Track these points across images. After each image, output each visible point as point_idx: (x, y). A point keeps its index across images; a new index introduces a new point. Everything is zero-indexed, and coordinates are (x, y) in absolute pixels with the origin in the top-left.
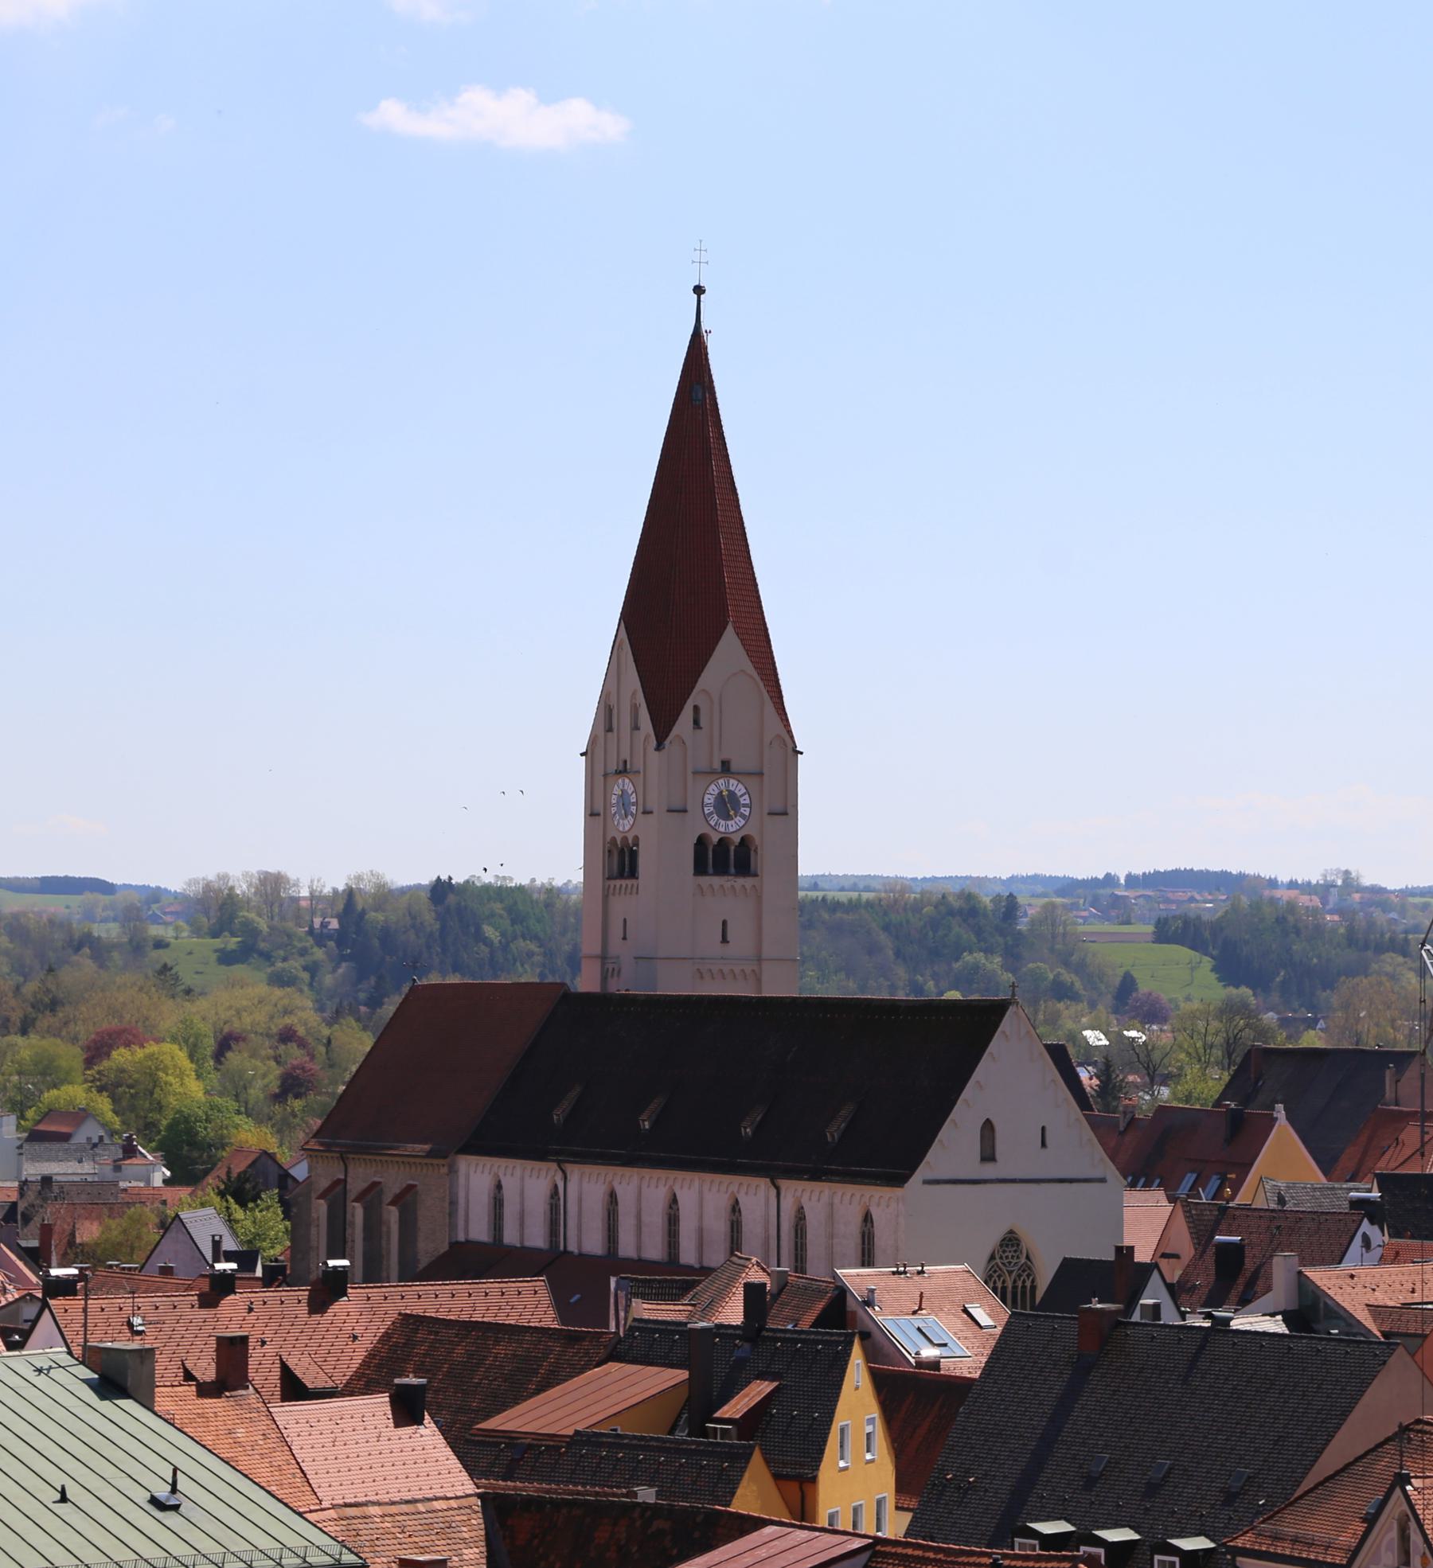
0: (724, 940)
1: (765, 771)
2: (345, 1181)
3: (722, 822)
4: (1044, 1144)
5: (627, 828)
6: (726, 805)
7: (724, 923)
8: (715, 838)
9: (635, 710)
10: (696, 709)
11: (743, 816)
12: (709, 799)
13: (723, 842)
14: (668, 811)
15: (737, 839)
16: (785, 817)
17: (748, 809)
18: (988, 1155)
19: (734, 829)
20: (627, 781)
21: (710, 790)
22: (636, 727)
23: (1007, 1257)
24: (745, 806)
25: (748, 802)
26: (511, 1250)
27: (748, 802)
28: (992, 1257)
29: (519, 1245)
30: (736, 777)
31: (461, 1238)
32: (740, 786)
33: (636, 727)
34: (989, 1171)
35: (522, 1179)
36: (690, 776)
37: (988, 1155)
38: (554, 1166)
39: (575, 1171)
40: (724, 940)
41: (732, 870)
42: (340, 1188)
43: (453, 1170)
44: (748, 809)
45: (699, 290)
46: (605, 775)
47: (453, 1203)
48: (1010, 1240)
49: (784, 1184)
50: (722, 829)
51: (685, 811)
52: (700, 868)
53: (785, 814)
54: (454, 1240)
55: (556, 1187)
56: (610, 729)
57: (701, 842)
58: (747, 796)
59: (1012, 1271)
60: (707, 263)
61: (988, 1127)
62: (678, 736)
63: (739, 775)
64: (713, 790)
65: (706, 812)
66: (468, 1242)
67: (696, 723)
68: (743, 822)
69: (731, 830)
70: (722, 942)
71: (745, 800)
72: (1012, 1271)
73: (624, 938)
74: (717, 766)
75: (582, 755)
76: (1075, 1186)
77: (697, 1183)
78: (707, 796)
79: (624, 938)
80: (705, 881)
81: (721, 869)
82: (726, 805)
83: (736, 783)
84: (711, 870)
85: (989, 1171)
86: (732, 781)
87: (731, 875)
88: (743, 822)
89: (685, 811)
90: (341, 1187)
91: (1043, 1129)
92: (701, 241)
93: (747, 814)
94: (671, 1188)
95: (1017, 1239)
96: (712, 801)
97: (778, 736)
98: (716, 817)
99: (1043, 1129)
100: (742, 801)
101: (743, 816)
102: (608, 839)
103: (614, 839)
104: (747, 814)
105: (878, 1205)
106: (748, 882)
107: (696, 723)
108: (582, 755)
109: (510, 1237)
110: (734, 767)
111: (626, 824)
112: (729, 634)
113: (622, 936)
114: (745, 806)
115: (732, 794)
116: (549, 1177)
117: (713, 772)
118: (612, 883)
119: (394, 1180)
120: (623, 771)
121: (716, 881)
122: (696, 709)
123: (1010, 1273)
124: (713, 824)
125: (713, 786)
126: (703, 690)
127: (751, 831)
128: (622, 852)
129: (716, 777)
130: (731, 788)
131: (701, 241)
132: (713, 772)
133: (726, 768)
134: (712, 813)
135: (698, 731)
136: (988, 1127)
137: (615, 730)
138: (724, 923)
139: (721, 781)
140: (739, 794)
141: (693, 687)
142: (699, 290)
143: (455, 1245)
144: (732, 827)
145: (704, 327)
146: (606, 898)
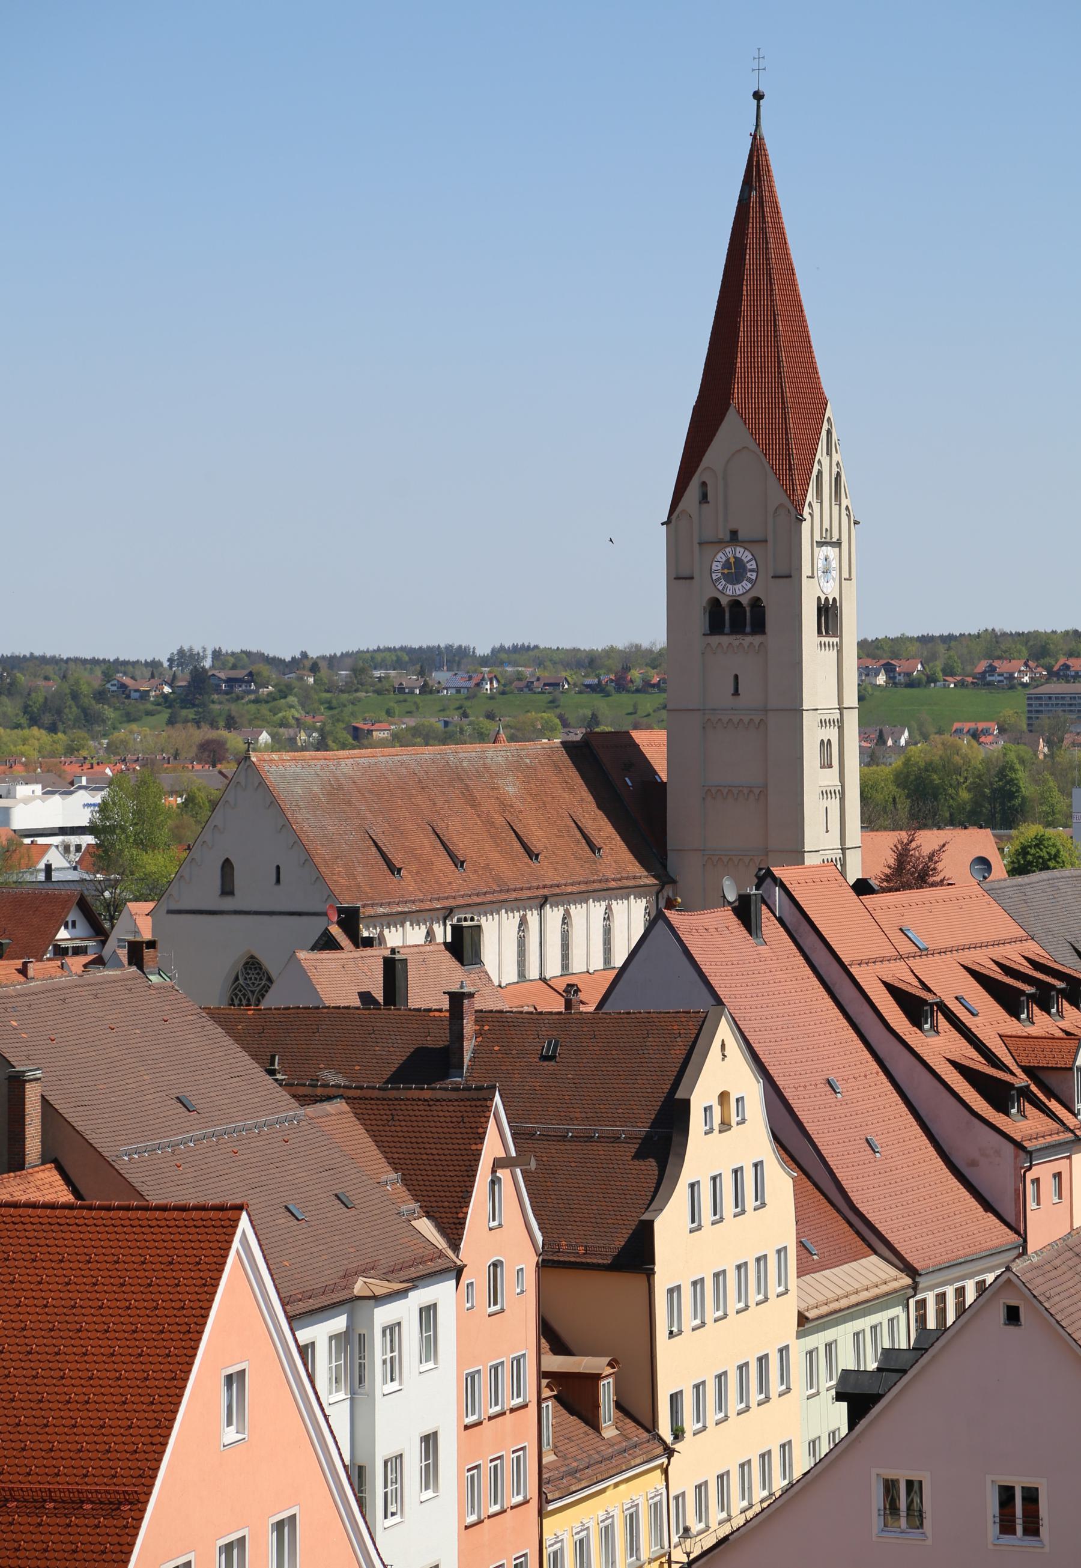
0: (736, 692)
1: (770, 538)
3: (730, 586)
4: (278, 881)
6: (735, 572)
7: (736, 677)
10: (704, 484)
11: (750, 580)
17: (755, 574)
18: (227, 891)
19: (741, 592)
21: (718, 558)
23: (251, 979)
24: (751, 570)
25: (754, 567)
28: (237, 979)
30: (745, 545)
32: (747, 553)
34: (228, 903)
37: (227, 891)
40: (736, 692)
41: (748, 629)
45: (758, 96)
48: (253, 964)
50: (730, 593)
51: (692, 578)
53: (790, 576)
57: (715, 603)
58: (753, 562)
59: (251, 991)
61: (227, 866)
63: (747, 544)
64: (721, 557)
65: (714, 578)
67: (704, 498)
68: (750, 585)
69: (738, 593)
70: (733, 695)
71: (752, 565)
72: (251, 991)
74: (724, 535)
76: (304, 919)
78: (715, 564)
80: (715, 640)
81: (738, 628)
82: (735, 572)
83: (742, 550)
84: (727, 629)
85: (228, 903)
86: (738, 549)
87: (726, 634)
88: (750, 585)
89: (692, 578)
91: (278, 868)
92: (759, 49)
95: (258, 964)
98: (724, 582)
99: (278, 868)
100: (749, 566)
101: (750, 580)
104: (754, 578)
106: (757, 639)
107: (704, 498)
110: (741, 536)
114: (751, 570)
115: (738, 561)
117: (720, 542)
121: (724, 640)
122: (704, 484)
123: (253, 992)
124: (721, 588)
125: (720, 554)
129: (724, 545)
130: (738, 555)
131: (759, 49)
132: (720, 542)
133: (734, 537)
134: (719, 579)
136: (227, 866)
138: (736, 677)
139: (728, 550)
140: (746, 560)
141: (698, 466)
142: (758, 96)
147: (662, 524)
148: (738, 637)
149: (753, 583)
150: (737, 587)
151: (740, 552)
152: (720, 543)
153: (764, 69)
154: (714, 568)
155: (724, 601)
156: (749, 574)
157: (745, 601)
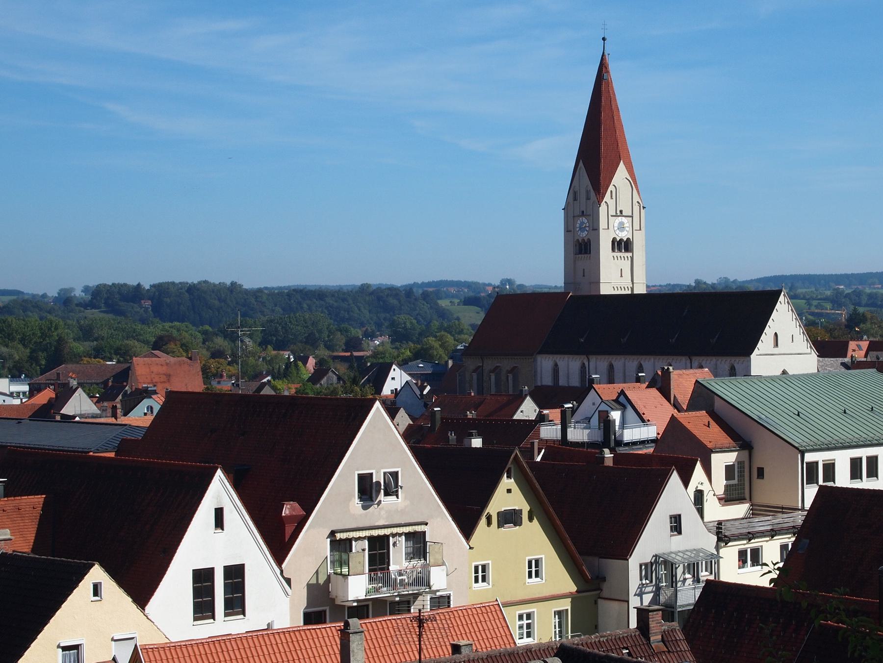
2: (483, 366)
5: (584, 236)
6: (621, 227)
8: (618, 240)
9: (588, 192)
10: (611, 191)
12: (616, 225)
13: (621, 240)
15: (625, 240)
18: (776, 345)
20: (584, 218)
22: (588, 198)
26: (564, 388)
29: (567, 385)
31: (539, 384)
33: (588, 198)
34: (776, 351)
35: (568, 361)
38: (585, 356)
39: (593, 359)
41: (623, 251)
42: (481, 368)
43: (535, 361)
46: (574, 217)
47: (536, 372)
49: (694, 358)
52: (613, 250)
54: (536, 385)
55: (584, 364)
56: (575, 199)
66: (542, 386)
73: (584, 276)
75: (563, 209)
77: (652, 360)
79: (584, 276)
80: (615, 254)
81: (620, 250)
82: (621, 227)
84: (616, 251)
85: (776, 351)
90: (481, 368)
93: (628, 230)
94: (639, 362)
97: (638, 202)
102: (575, 240)
103: (578, 240)
105: (738, 363)
106: (630, 254)
108: (563, 209)
109: (562, 382)
110: (624, 214)
111: (584, 234)
112: (622, 165)
113: (582, 275)
116: (581, 360)
118: (577, 256)
119: (506, 364)
120: (583, 214)
121: (619, 254)
122: (611, 191)
128: (580, 244)
137: (578, 199)
142: (604, 39)
143: (535, 387)
144: (624, 235)
145: (606, 54)
146: (575, 262)
151: (624, 219)
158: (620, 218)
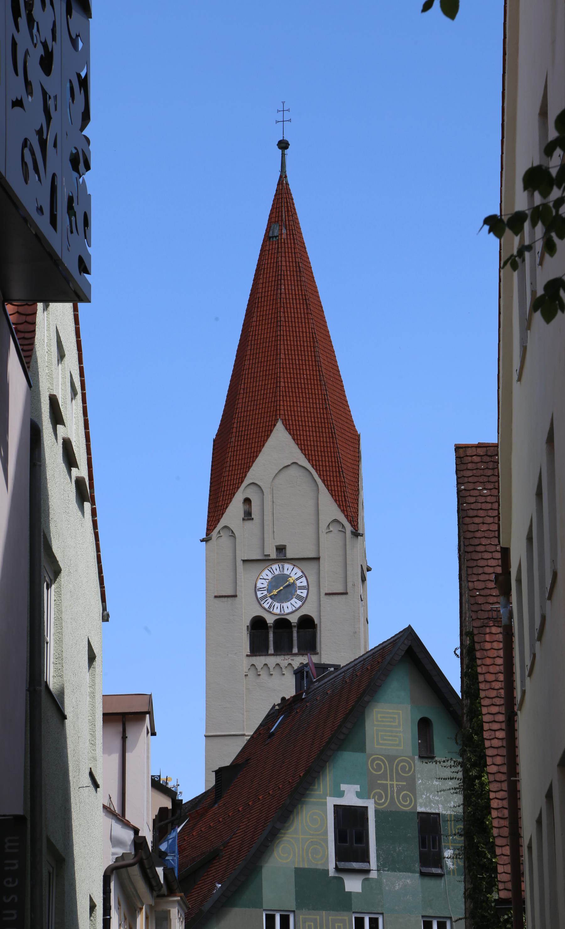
10: (247, 501)
11: (299, 598)
12: (262, 584)
14: (216, 597)
16: (344, 597)
17: (305, 592)
19: (290, 610)
21: (264, 575)
24: (301, 588)
25: (305, 584)
27: (305, 584)
32: (296, 570)
36: (240, 564)
44: (305, 592)
45: (283, 145)
50: (277, 611)
51: (235, 596)
58: (304, 579)
60: (283, 103)
62: (226, 527)
64: (267, 574)
67: (248, 516)
68: (299, 603)
69: (287, 611)
78: (260, 581)
83: (291, 567)
86: (287, 566)
88: (299, 603)
93: (304, 595)
96: (266, 585)
101: (299, 598)
104: (304, 595)
110: (289, 555)
114: (301, 588)
122: (247, 501)
124: (266, 606)
125: (266, 572)
126: (253, 483)
127: (309, 610)
134: (265, 597)
135: (248, 523)
142: (283, 145)
147: (202, 541)
148: (287, 657)
149: (303, 600)
150: (285, 605)
151: (288, 568)
152: (266, 561)
153: (290, 121)
154: (259, 585)
155: (270, 620)
156: (299, 592)
157: (294, 619)
158: (275, 567)
